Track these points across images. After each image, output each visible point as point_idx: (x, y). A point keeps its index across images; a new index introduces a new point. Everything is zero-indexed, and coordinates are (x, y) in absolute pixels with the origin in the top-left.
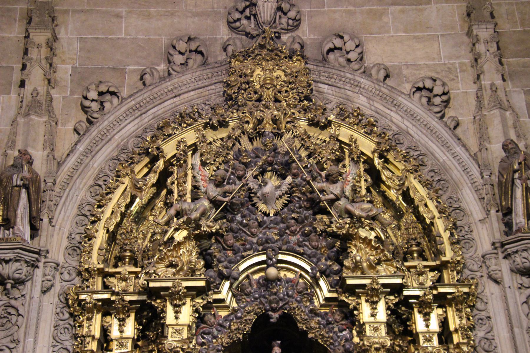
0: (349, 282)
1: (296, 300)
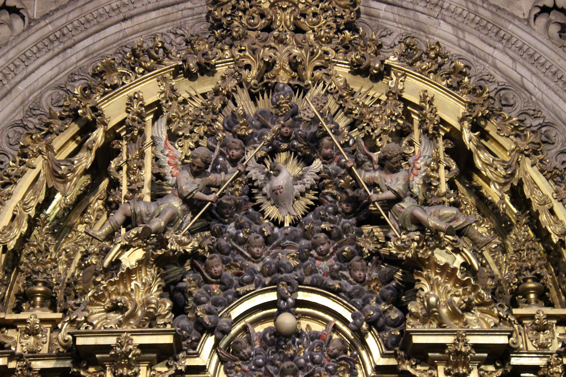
0: (417, 339)
1: (327, 370)
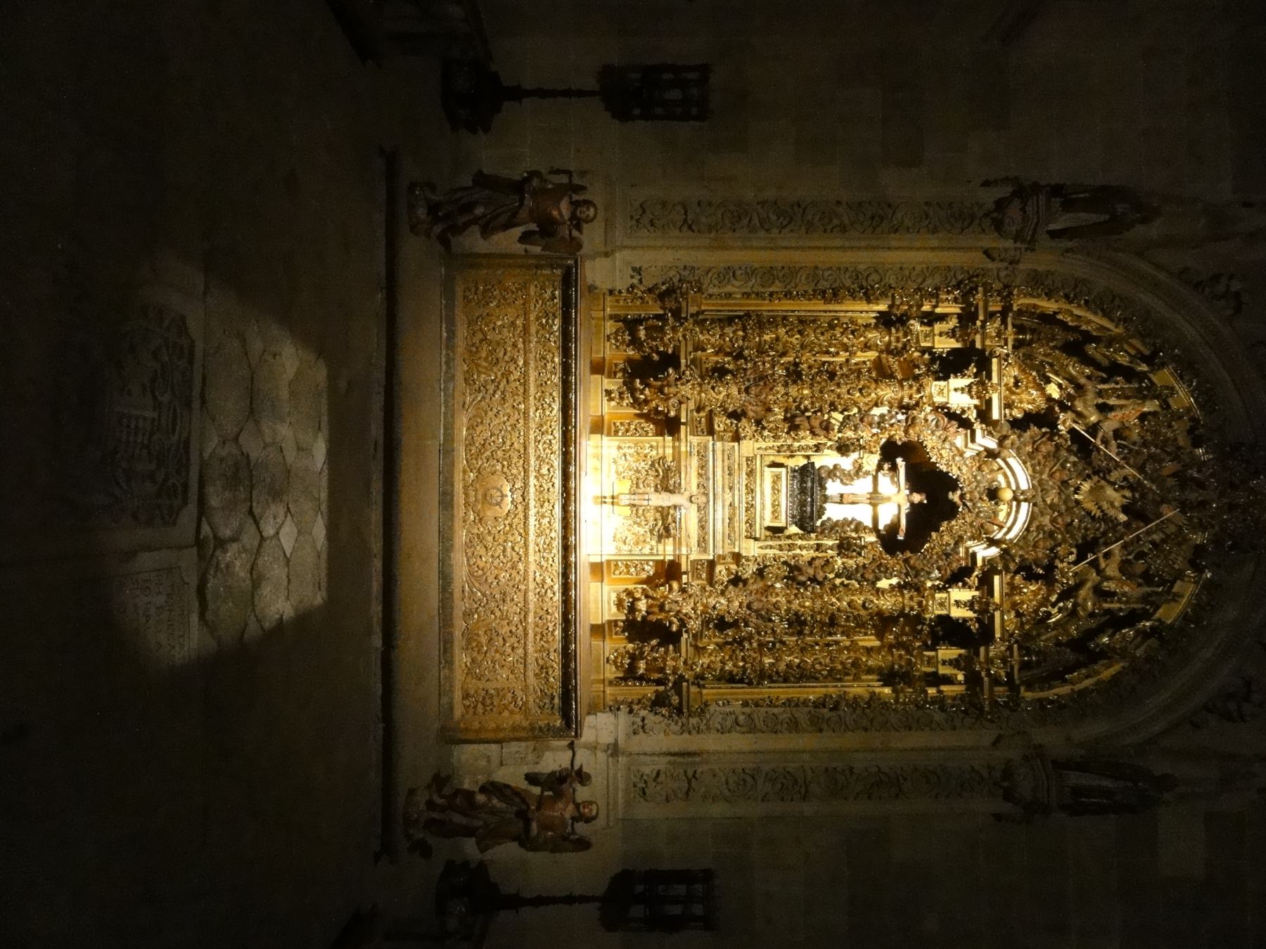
0: (997, 579)
1: (972, 522)
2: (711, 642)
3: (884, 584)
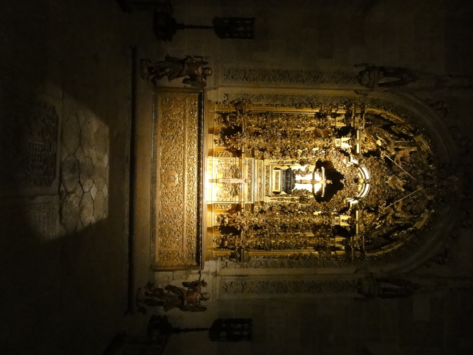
0: (357, 212)
1: (349, 191)
2: (252, 234)
3: (316, 213)
